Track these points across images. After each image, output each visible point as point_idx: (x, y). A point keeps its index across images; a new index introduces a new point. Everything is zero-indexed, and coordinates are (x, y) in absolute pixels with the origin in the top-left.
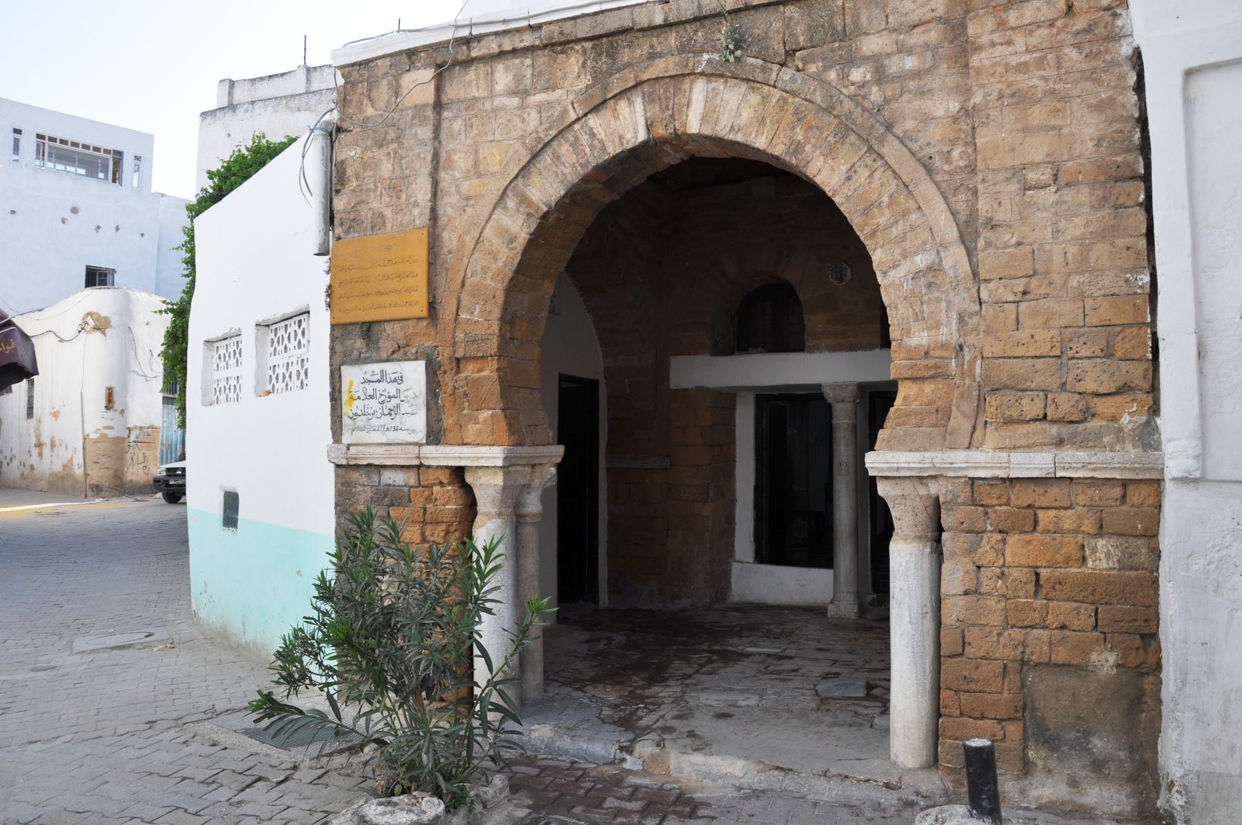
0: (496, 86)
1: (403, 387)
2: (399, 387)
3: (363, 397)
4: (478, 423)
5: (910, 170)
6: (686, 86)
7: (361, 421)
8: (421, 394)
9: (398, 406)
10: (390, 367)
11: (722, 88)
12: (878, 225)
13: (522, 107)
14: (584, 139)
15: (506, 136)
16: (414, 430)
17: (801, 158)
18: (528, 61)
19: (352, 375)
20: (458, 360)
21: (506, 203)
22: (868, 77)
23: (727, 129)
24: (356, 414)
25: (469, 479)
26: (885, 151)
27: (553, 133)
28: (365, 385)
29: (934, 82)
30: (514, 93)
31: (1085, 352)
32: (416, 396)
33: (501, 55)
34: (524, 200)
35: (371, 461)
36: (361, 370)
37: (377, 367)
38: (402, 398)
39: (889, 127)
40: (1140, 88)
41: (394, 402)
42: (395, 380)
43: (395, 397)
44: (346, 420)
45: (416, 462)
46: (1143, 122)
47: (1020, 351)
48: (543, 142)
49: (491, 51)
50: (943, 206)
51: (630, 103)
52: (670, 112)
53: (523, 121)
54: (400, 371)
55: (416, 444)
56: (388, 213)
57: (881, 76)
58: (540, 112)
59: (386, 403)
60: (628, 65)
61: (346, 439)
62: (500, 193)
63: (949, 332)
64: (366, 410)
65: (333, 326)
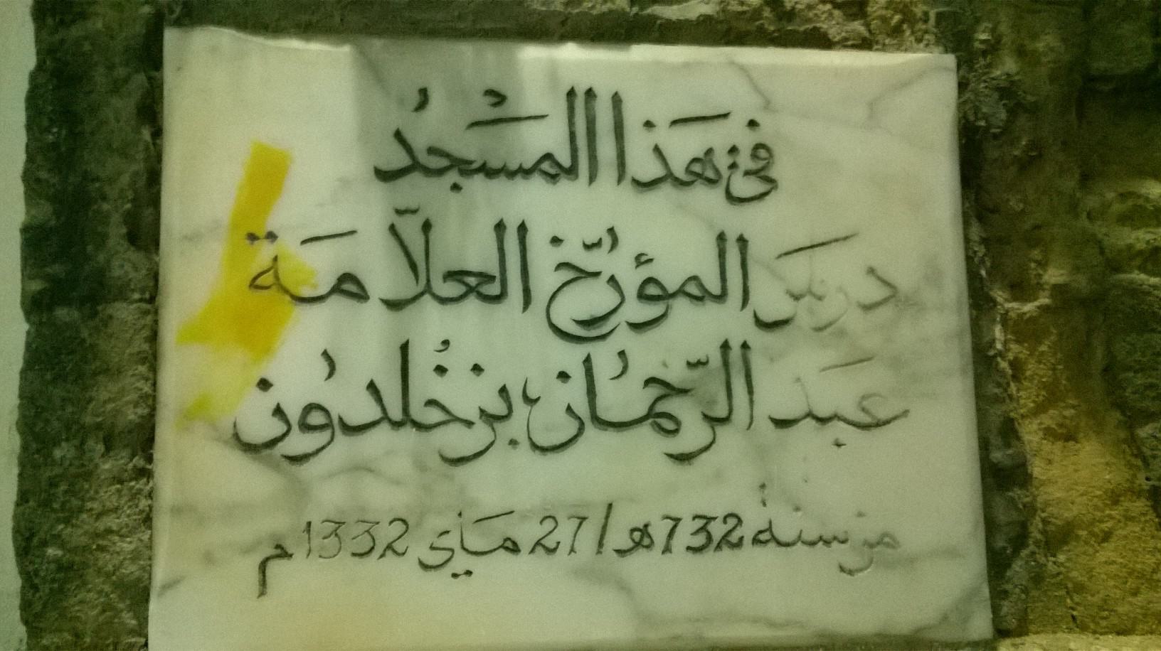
2: (737, 221)
8: (933, 277)
16: (885, 541)
28: (415, 190)
32: (893, 294)
38: (771, 302)
54: (743, 103)
59: (623, 339)
64: (425, 384)
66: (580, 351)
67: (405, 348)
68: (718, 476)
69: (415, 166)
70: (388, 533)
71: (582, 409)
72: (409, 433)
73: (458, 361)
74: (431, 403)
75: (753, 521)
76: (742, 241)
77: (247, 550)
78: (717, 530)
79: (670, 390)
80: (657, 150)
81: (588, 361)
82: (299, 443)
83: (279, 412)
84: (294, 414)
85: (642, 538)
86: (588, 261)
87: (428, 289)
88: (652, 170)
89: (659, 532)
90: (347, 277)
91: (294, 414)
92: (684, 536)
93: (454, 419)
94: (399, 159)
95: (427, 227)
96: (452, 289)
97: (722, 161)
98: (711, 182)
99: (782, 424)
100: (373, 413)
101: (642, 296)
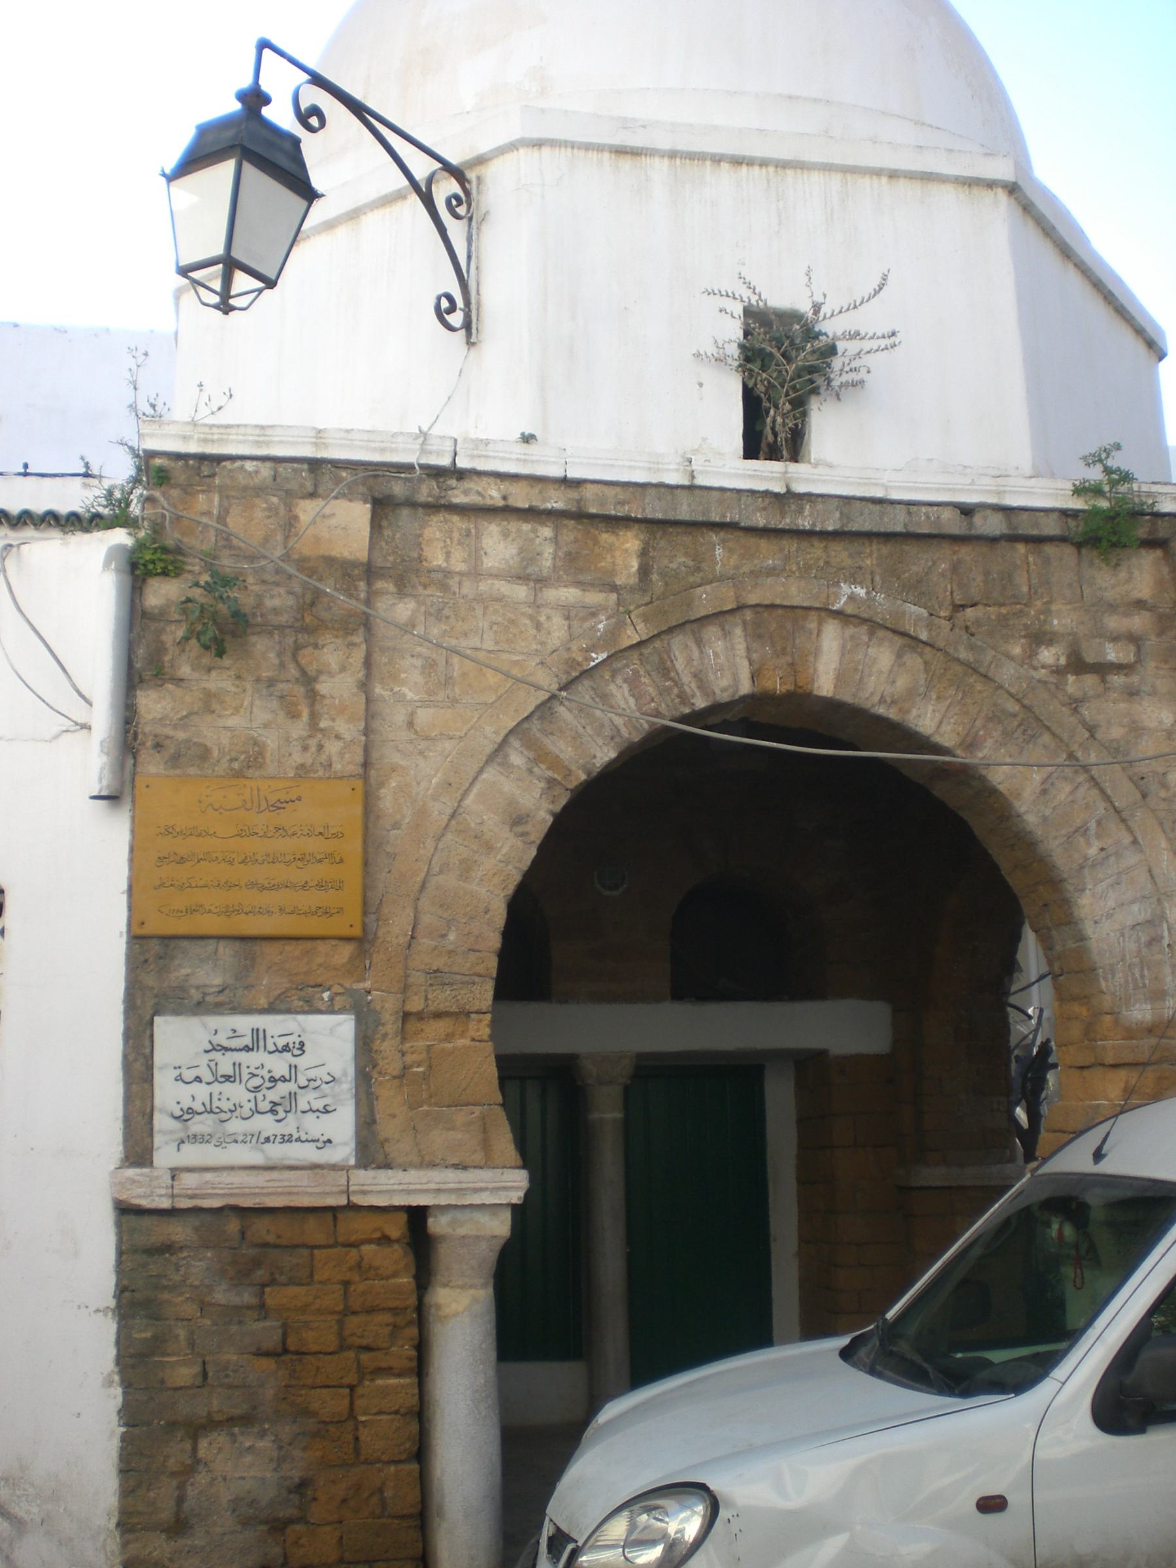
0: (485, 560)
1: (302, 1062)
2: (294, 1061)
3: (208, 1076)
4: (453, 1129)
6: (812, 625)
7: (199, 1125)
8: (345, 1074)
9: (293, 1096)
10: (276, 1025)
11: (865, 638)
12: (1086, 858)
13: (536, 605)
15: (506, 647)
16: (329, 1141)
17: (980, 755)
18: (546, 532)
20: (406, 1016)
21: (506, 756)
22: (1063, 661)
23: (876, 699)
24: (191, 1111)
28: (213, 1055)
30: (522, 578)
33: (507, 511)
35: (232, 1201)
36: (205, 1025)
37: (244, 1023)
38: (302, 1081)
39: (1092, 730)
41: (283, 1089)
42: (286, 1048)
43: (284, 1079)
44: (161, 1121)
45: (343, 1201)
48: (580, 669)
49: (489, 502)
51: (726, 634)
52: (789, 659)
53: (538, 626)
54: (297, 1030)
55: (334, 1167)
58: (567, 618)
59: (264, 1091)
61: (165, 1155)
62: (499, 739)
64: (216, 1103)
66: (253, 1095)
67: (211, 1094)
68: (287, 1125)
69: (214, 1049)
70: (207, 1138)
71: (254, 1108)
72: (212, 1115)
73: (224, 1098)
74: (218, 1107)
75: (295, 1136)
76: (296, 1067)
77: (175, 1141)
78: (286, 1138)
79: (275, 1104)
80: (275, 1044)
81: (255, 1097)
82: (186, 1117)
83: (182, 1109)
84: (185, 1109)
85: (267, 1140)
86: (256, 1072)
87: (216, 1080)
88: (273, 1048)
89: (272, 1138)
90: (197, 1077)
91: (185, 1109)
92: (278, 1139)
93: (222, 1111)
94: (210, 1047)
95: (216, 1064)
96: (223, 1079)
97: (291, 1046)
98: (289, 1051)
99: (304, 1112)
100: (203, 1110)
101: (270, 1081)
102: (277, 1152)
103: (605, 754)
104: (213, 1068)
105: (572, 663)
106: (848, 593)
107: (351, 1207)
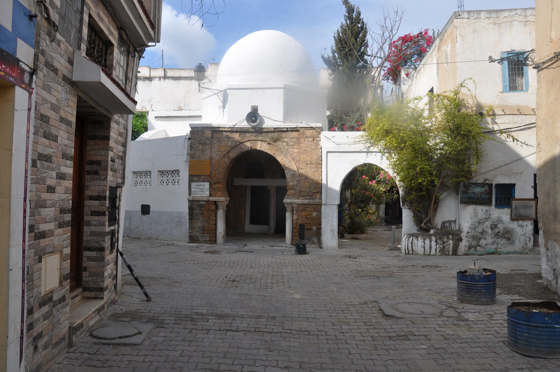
1: (204, 187)
5: (290, 159)
10: (202, 183)
13: (228, 141)
14: (239, 148)
19: (193, 185)
25: (217, 203)
26: (288, 156)
27: (234, 146)
29: (295, 147)
31: (313, 187)
34: (228, 157)
37: (199, 183)
40: (321, 152)
44: (192, 192)
46: (321, 157)
47: (304, 186)
50: (295, 165)
56: (201, 156)
57: (287, 145)
60: (247, 137)
61: (192, 196)
63: (295, 183)
65: (189, 175)
102: (202, 195)
103: (235, 156)
104: (196, 187)
105: (231, 147)
106: (260, 138)
107: (208, 201)
